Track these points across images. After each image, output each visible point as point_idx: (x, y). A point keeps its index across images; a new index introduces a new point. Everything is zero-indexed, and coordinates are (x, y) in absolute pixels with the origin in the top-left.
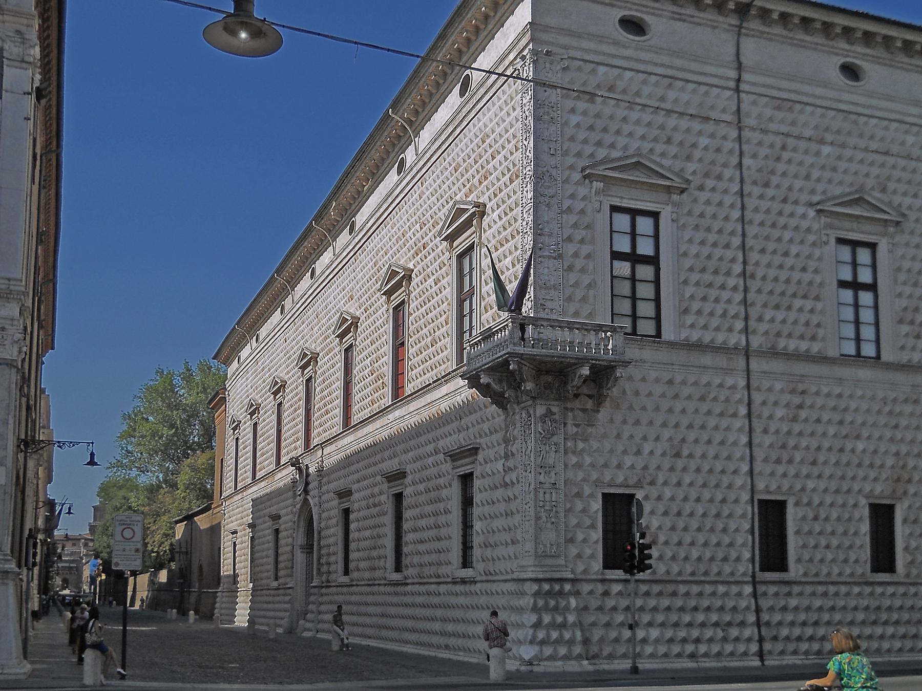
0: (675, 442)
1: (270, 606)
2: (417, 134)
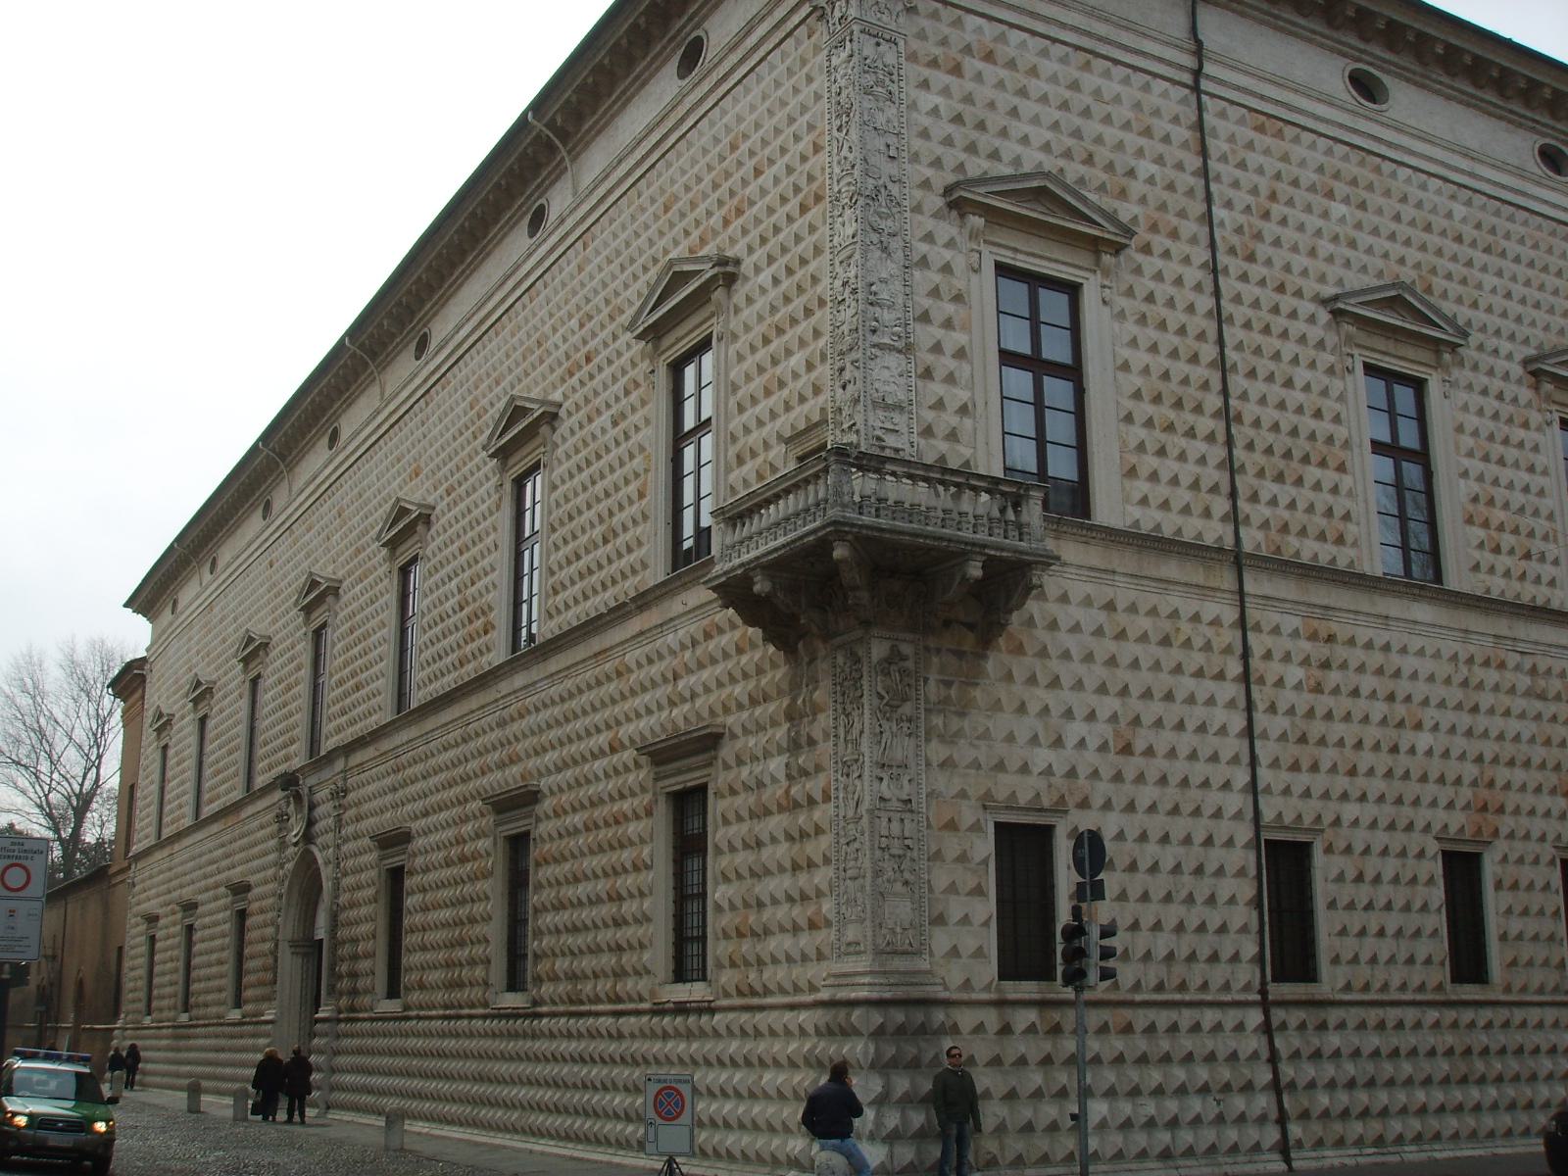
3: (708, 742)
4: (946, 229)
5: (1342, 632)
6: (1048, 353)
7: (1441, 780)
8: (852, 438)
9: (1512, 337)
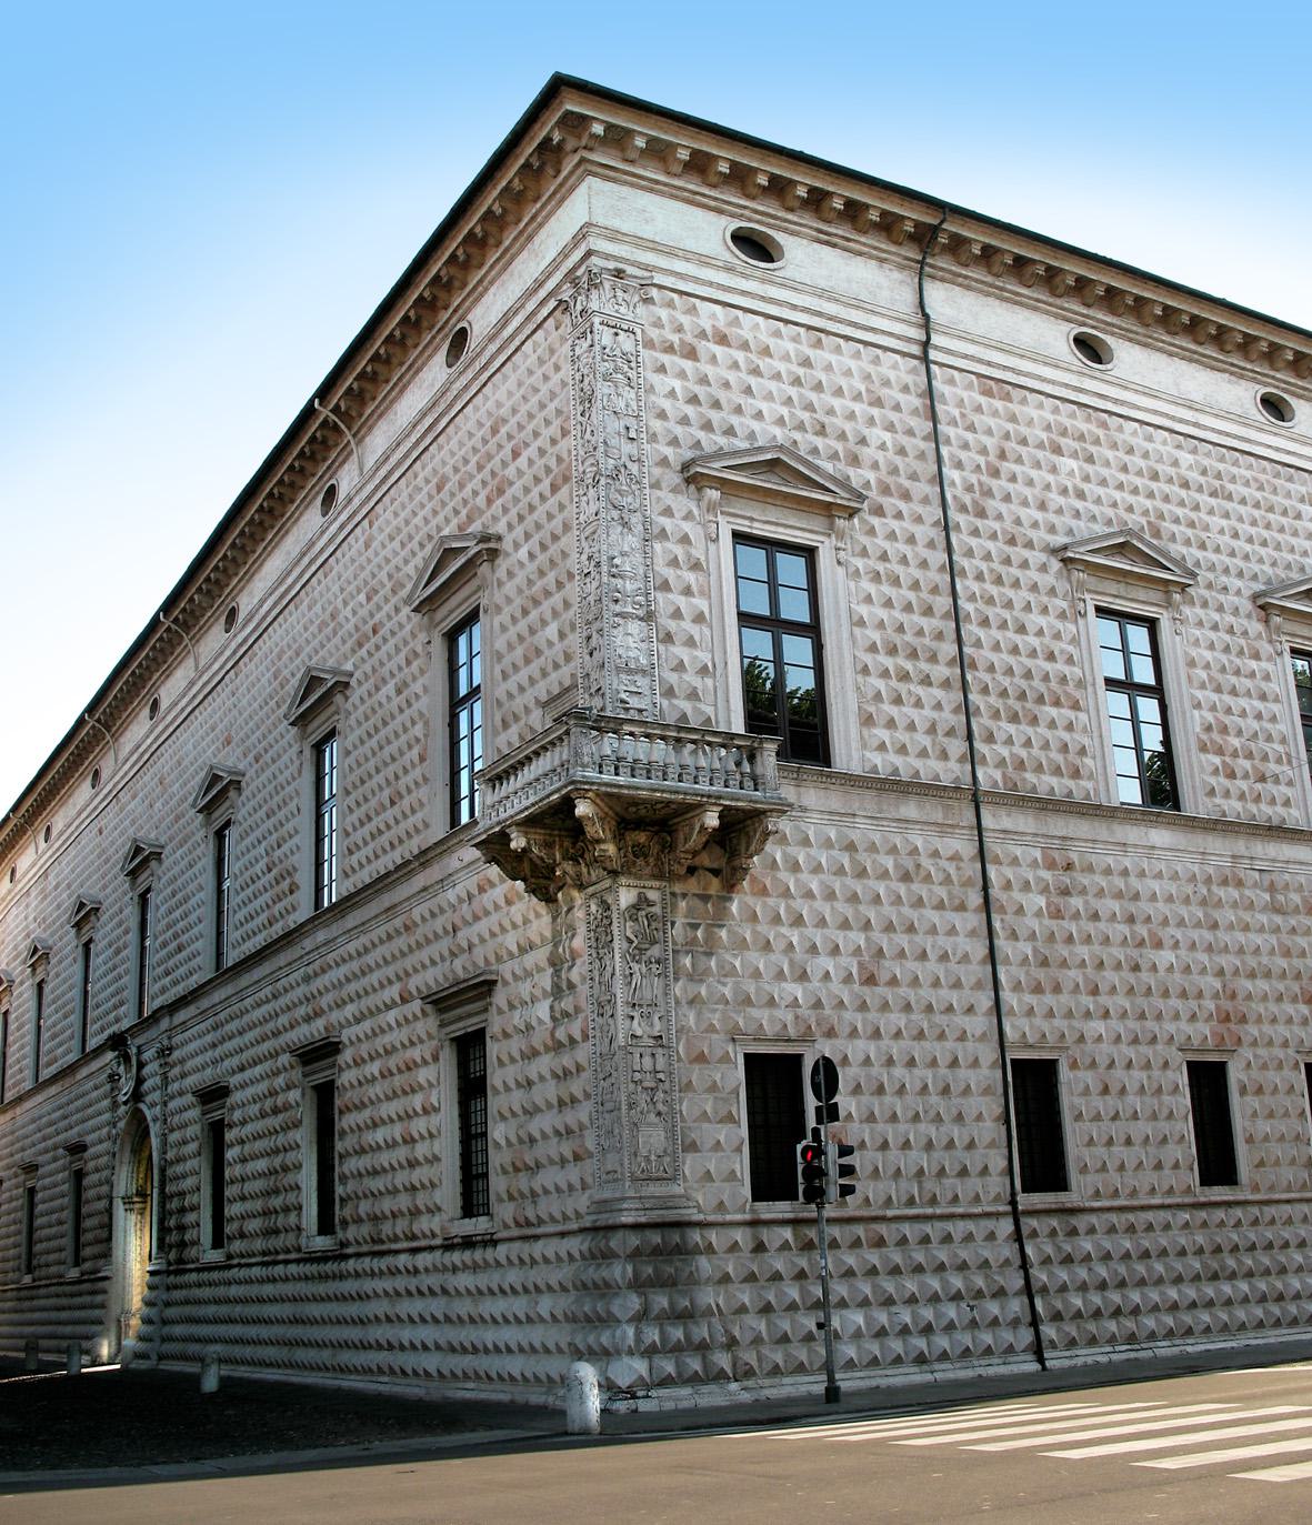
1: (64, 1315)
3: (483, 988)
6: (788, 613)
8: (597, 702)
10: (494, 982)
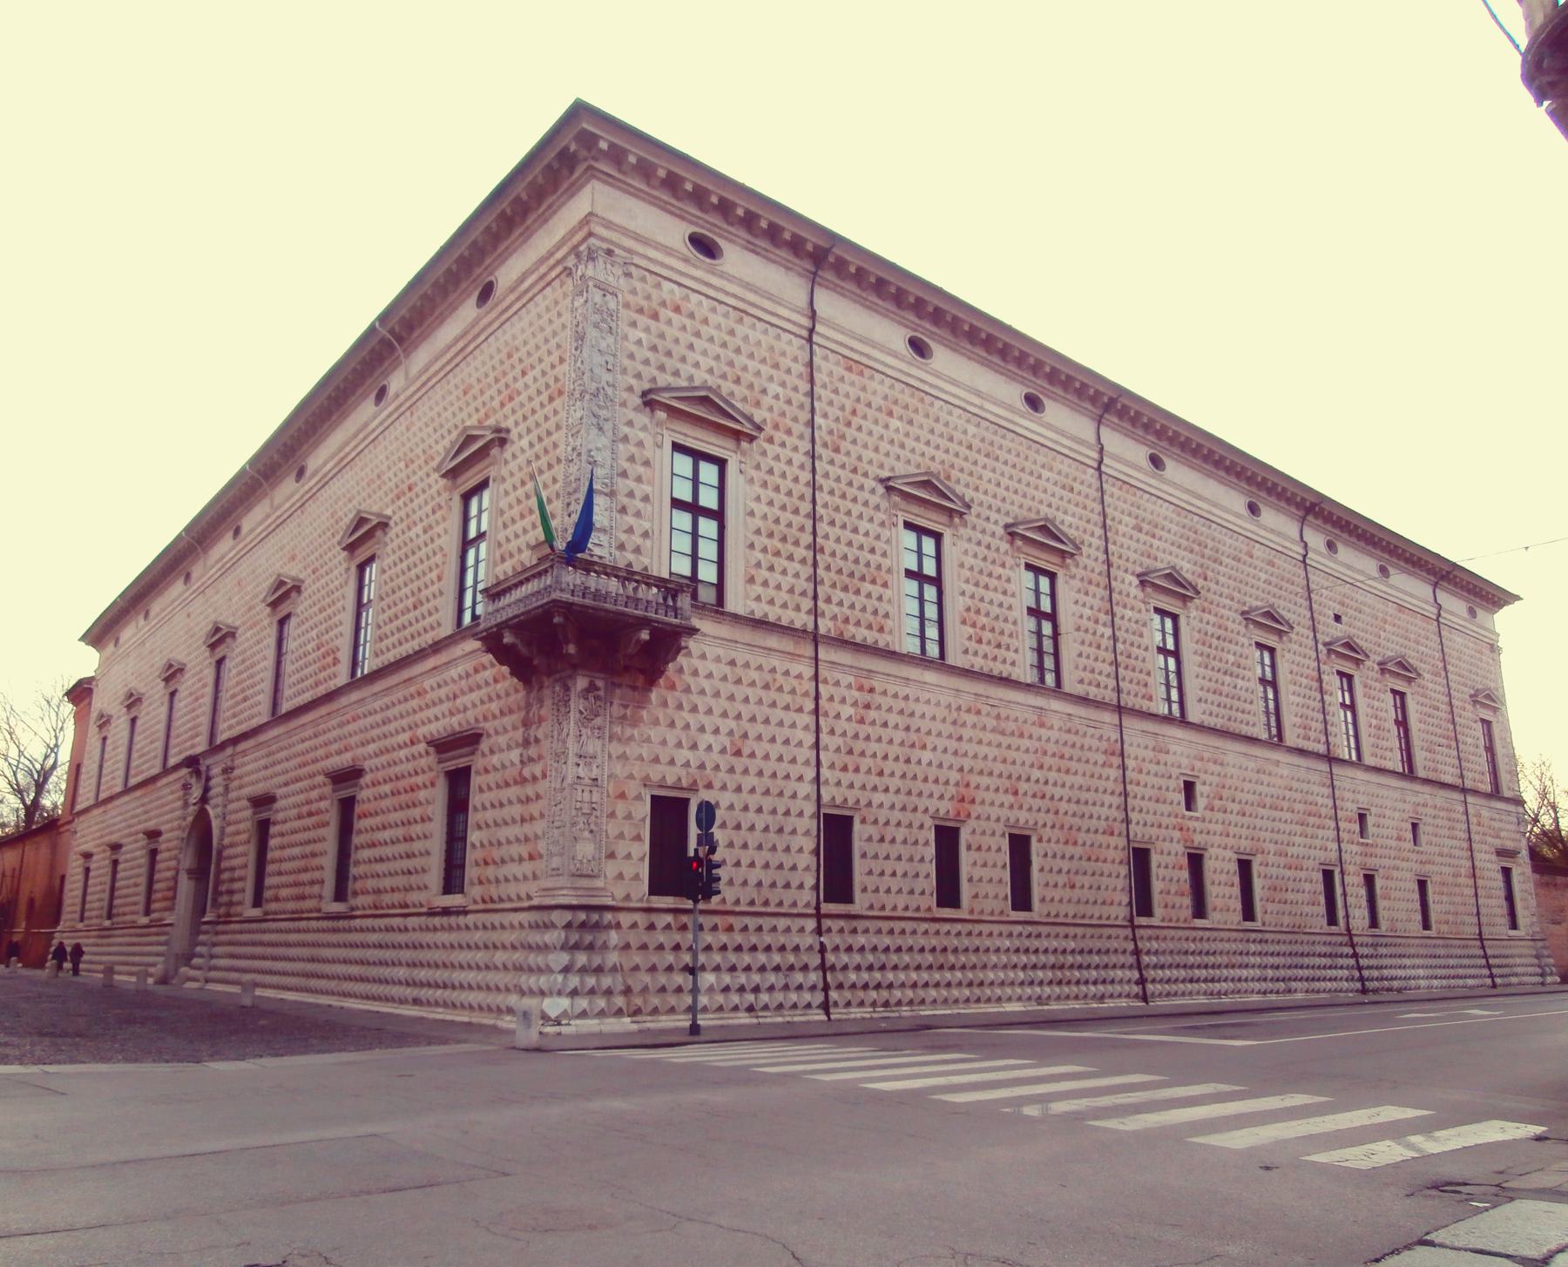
0: (737, 736)
1: (137, 949)
2: (407, 353)
3: (470, 740)
4: (643, 419)
5: (878, 686)
7: (936, 781)
9: (999, 511)
10: (480, 735)
